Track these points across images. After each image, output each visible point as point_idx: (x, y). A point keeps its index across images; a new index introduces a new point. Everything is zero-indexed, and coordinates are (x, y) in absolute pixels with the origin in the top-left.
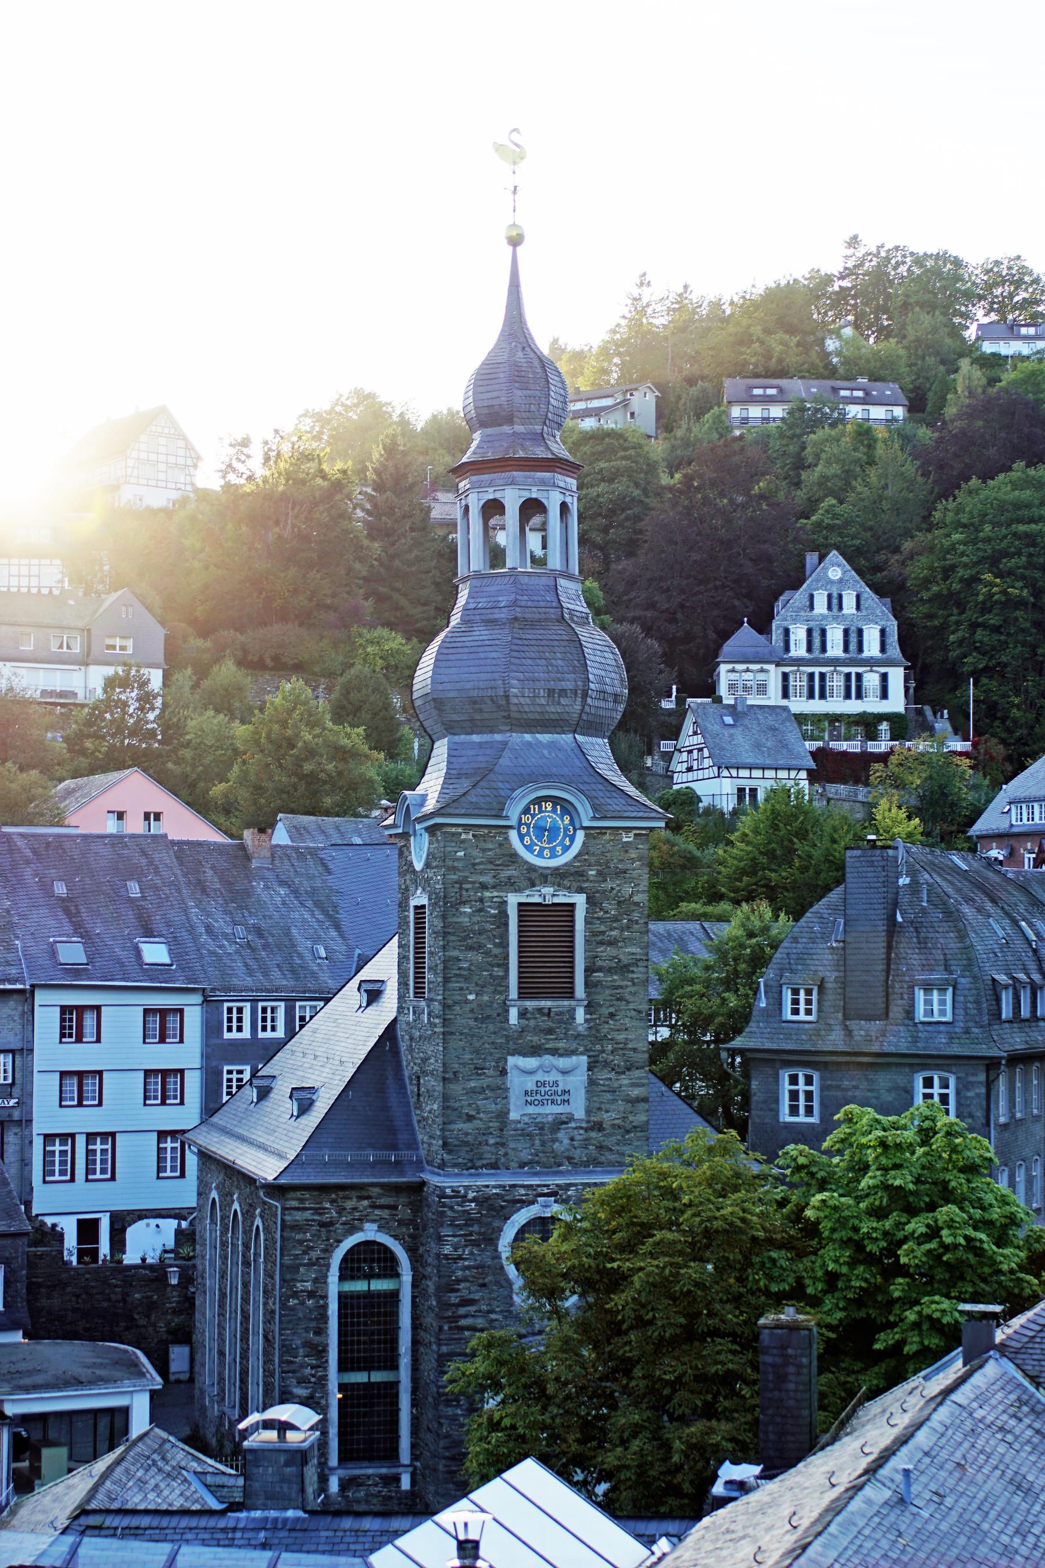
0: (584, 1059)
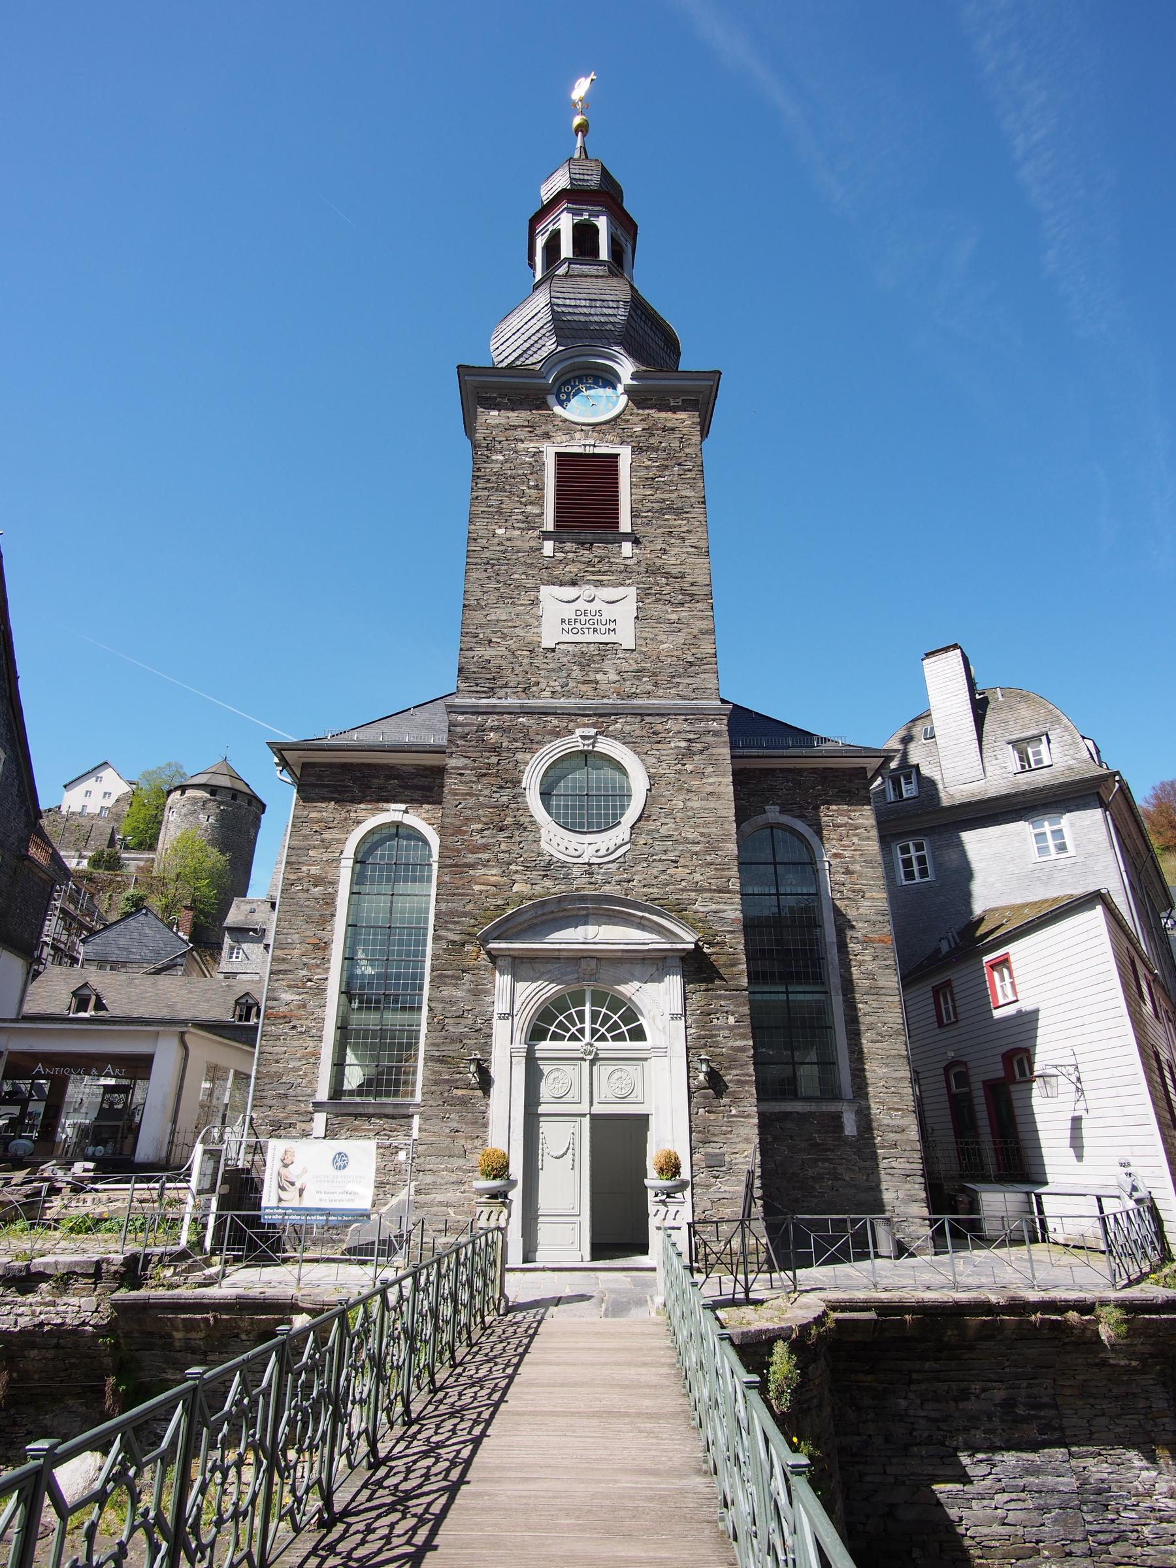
0: (632, 591)
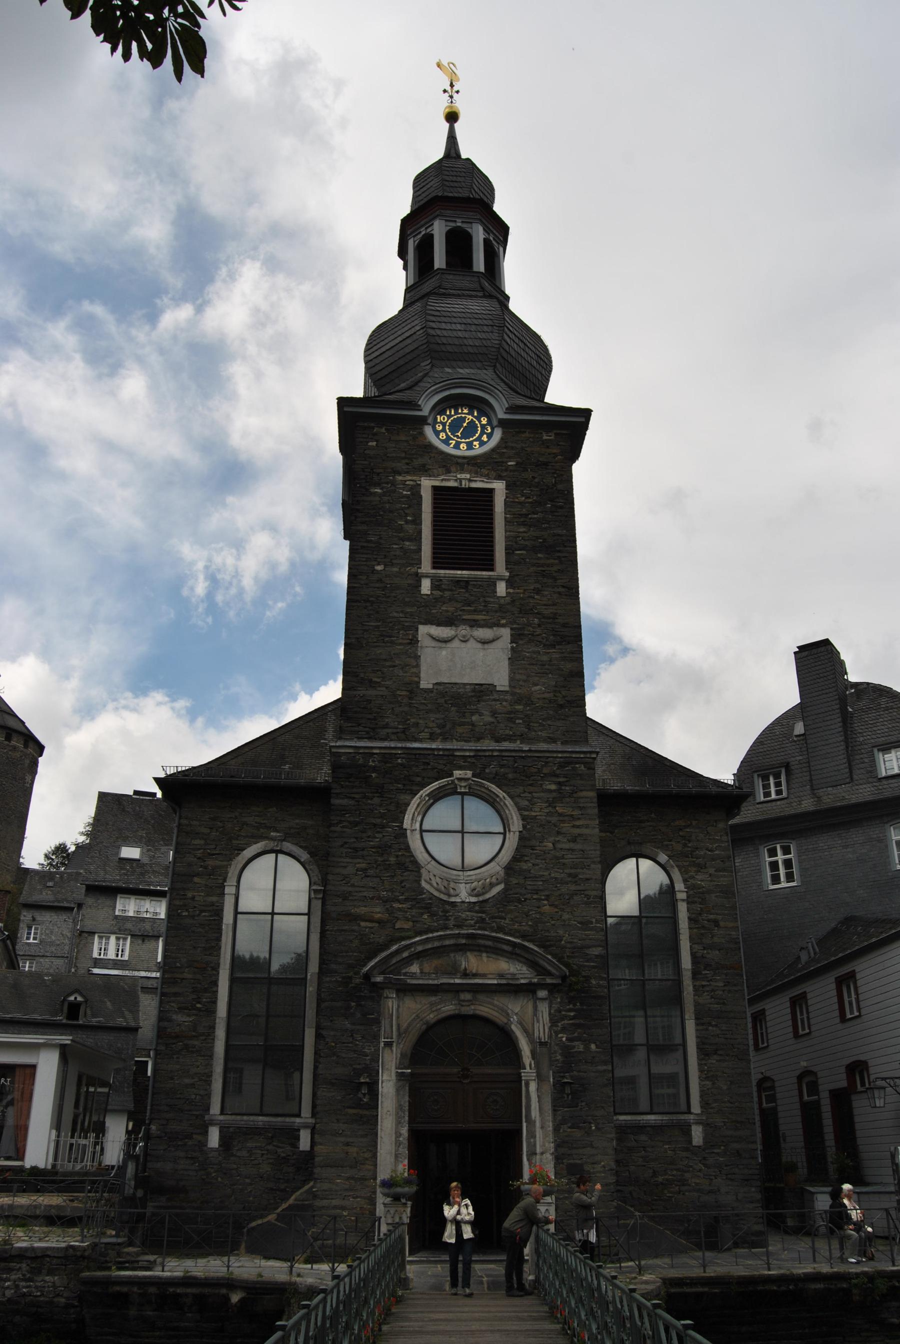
0: (506, 633)
